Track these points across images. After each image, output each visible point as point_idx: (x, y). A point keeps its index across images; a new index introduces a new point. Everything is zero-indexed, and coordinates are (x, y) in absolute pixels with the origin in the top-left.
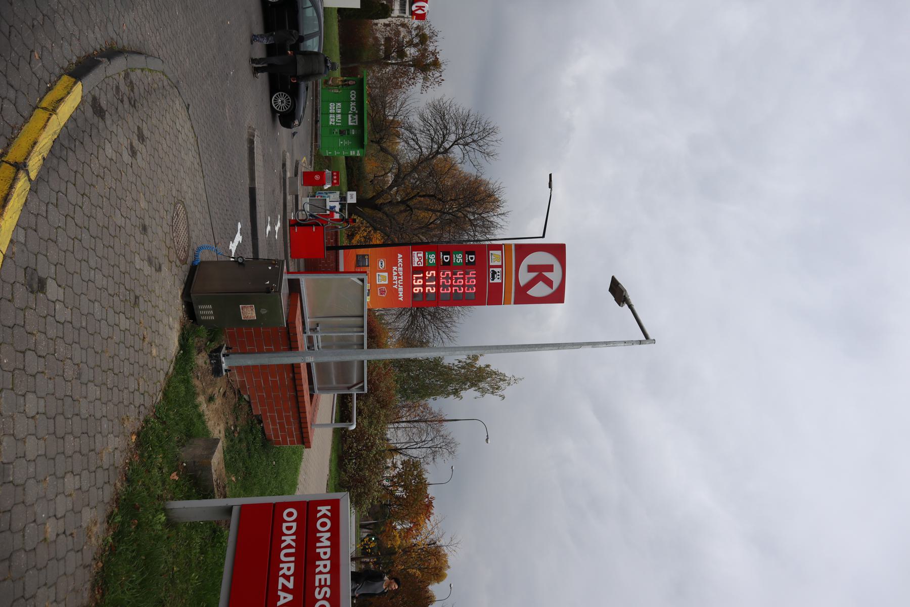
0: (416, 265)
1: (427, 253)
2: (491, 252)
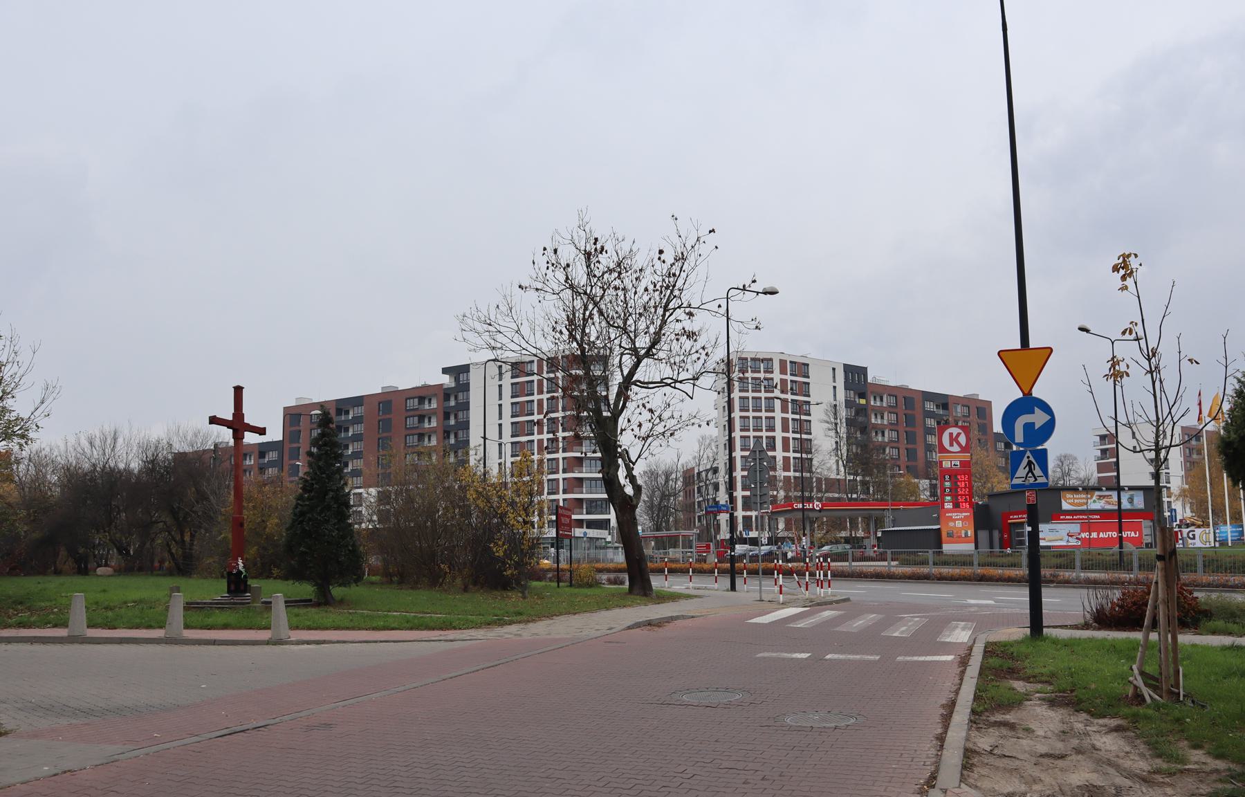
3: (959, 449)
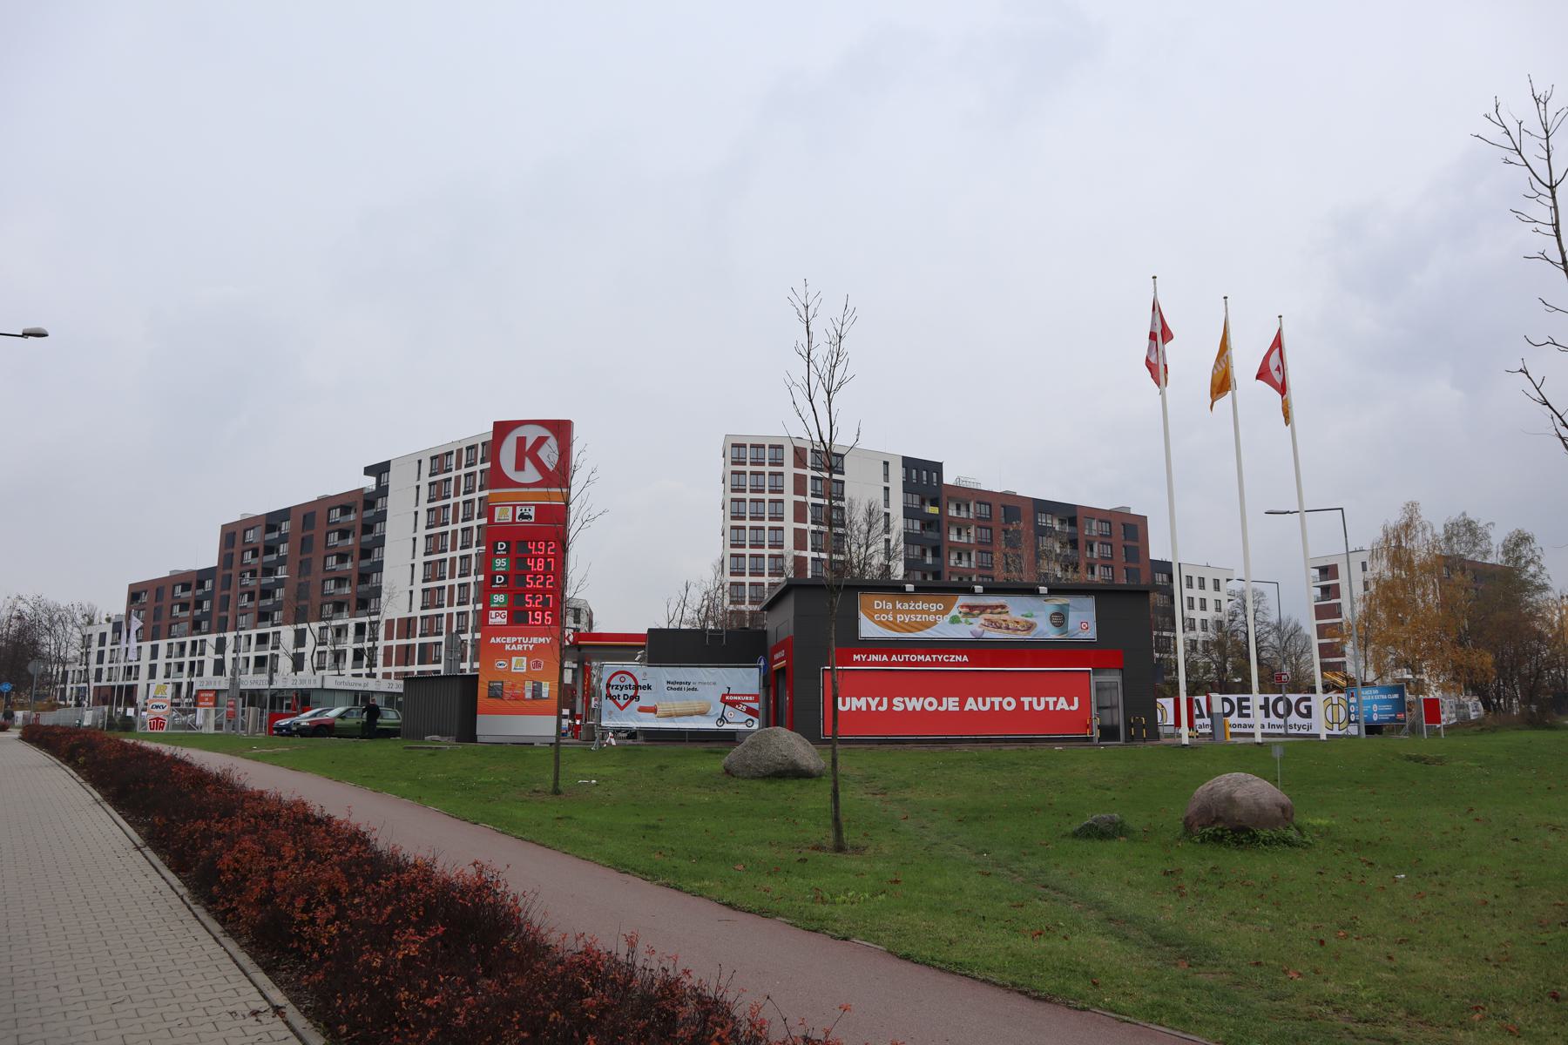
0: (505, 620)
1: (492, 605)
2: (496, 521)
3: (538, 478)
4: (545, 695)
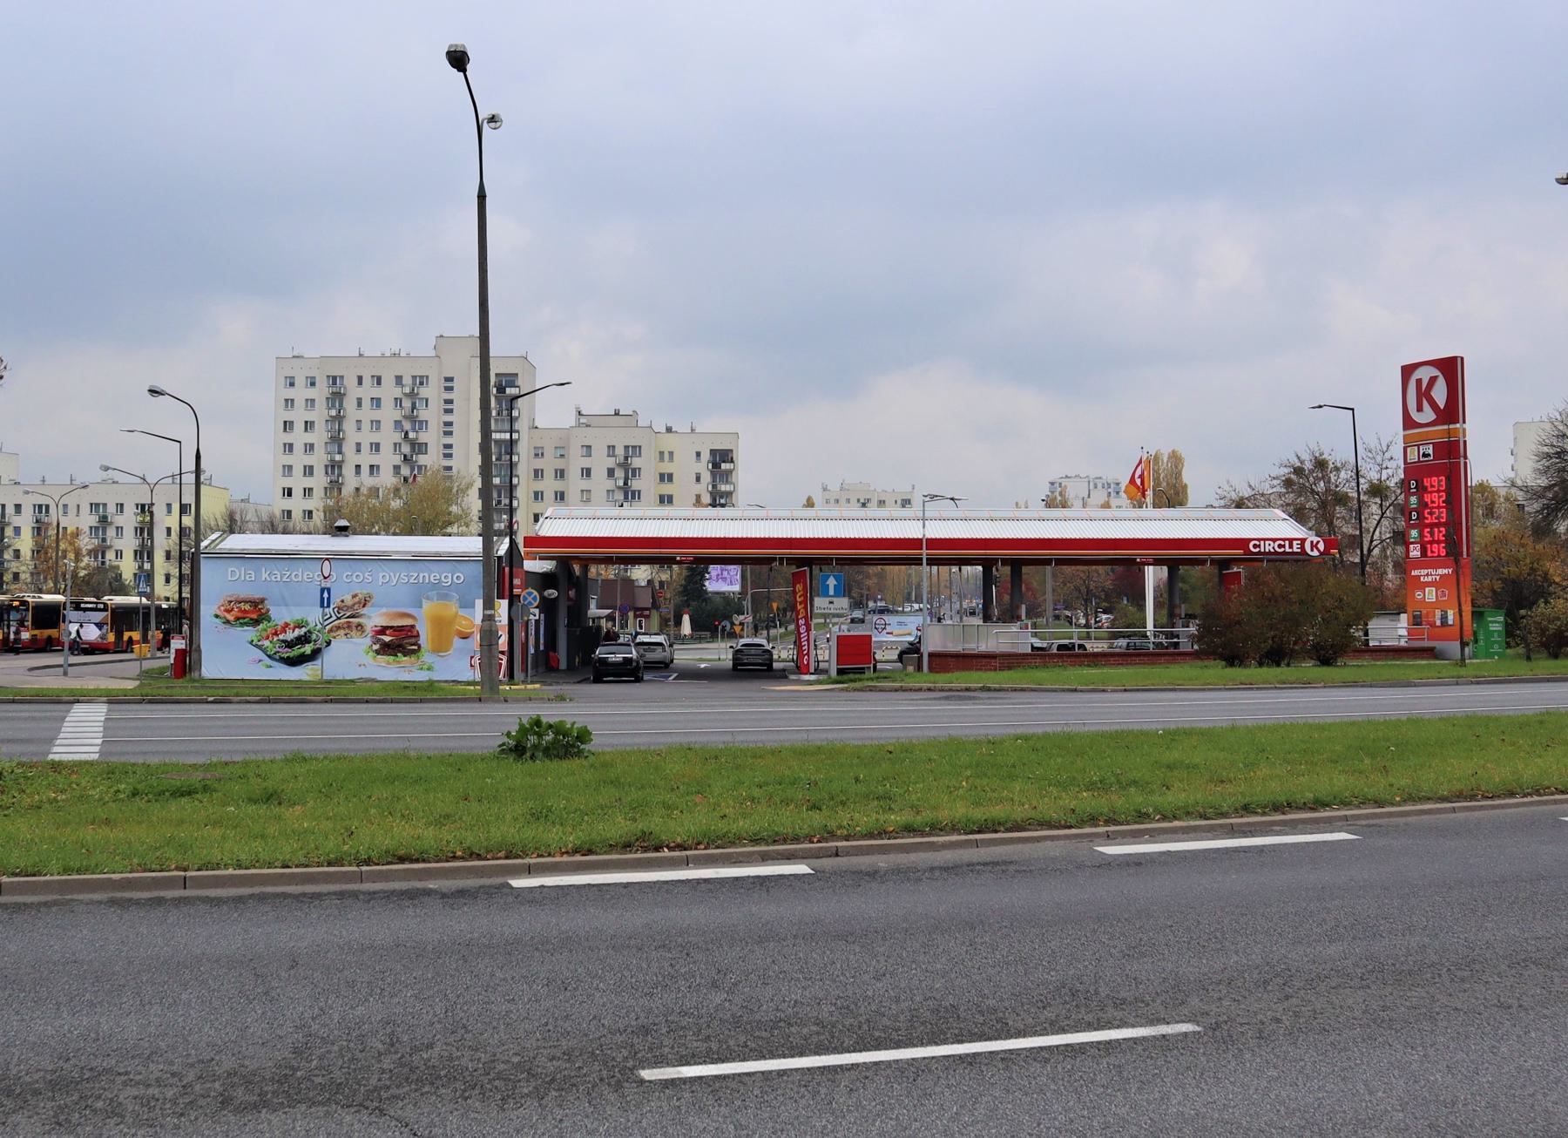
0: (1419, 553)
4: (1450, 622)
